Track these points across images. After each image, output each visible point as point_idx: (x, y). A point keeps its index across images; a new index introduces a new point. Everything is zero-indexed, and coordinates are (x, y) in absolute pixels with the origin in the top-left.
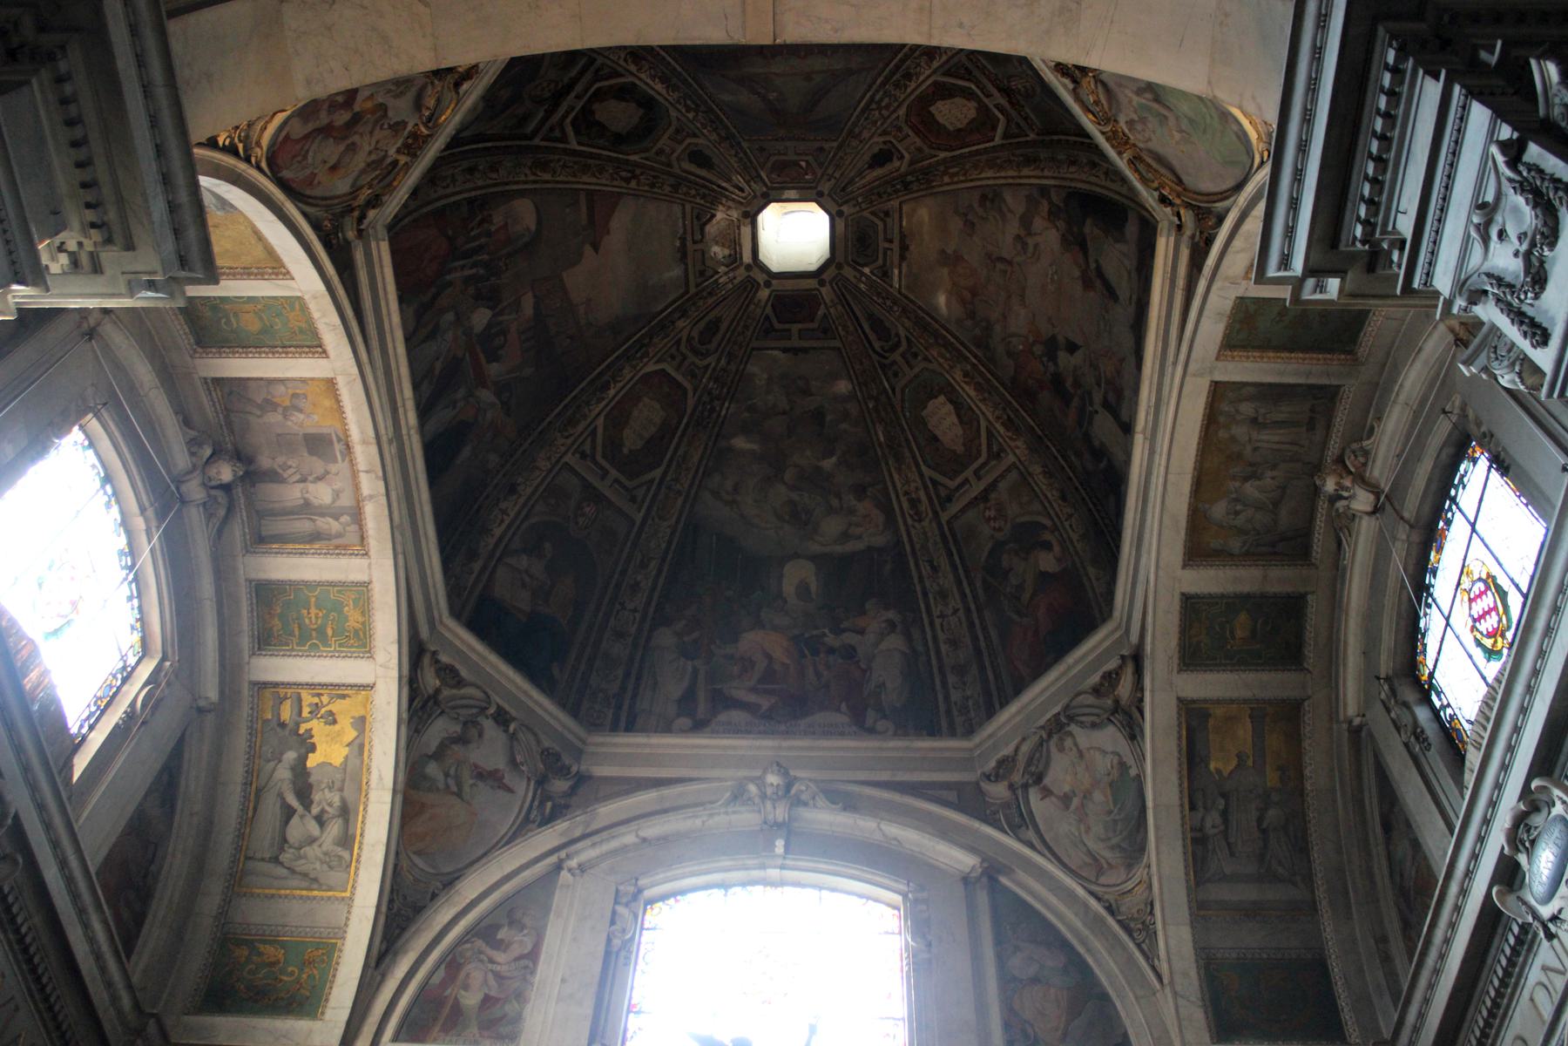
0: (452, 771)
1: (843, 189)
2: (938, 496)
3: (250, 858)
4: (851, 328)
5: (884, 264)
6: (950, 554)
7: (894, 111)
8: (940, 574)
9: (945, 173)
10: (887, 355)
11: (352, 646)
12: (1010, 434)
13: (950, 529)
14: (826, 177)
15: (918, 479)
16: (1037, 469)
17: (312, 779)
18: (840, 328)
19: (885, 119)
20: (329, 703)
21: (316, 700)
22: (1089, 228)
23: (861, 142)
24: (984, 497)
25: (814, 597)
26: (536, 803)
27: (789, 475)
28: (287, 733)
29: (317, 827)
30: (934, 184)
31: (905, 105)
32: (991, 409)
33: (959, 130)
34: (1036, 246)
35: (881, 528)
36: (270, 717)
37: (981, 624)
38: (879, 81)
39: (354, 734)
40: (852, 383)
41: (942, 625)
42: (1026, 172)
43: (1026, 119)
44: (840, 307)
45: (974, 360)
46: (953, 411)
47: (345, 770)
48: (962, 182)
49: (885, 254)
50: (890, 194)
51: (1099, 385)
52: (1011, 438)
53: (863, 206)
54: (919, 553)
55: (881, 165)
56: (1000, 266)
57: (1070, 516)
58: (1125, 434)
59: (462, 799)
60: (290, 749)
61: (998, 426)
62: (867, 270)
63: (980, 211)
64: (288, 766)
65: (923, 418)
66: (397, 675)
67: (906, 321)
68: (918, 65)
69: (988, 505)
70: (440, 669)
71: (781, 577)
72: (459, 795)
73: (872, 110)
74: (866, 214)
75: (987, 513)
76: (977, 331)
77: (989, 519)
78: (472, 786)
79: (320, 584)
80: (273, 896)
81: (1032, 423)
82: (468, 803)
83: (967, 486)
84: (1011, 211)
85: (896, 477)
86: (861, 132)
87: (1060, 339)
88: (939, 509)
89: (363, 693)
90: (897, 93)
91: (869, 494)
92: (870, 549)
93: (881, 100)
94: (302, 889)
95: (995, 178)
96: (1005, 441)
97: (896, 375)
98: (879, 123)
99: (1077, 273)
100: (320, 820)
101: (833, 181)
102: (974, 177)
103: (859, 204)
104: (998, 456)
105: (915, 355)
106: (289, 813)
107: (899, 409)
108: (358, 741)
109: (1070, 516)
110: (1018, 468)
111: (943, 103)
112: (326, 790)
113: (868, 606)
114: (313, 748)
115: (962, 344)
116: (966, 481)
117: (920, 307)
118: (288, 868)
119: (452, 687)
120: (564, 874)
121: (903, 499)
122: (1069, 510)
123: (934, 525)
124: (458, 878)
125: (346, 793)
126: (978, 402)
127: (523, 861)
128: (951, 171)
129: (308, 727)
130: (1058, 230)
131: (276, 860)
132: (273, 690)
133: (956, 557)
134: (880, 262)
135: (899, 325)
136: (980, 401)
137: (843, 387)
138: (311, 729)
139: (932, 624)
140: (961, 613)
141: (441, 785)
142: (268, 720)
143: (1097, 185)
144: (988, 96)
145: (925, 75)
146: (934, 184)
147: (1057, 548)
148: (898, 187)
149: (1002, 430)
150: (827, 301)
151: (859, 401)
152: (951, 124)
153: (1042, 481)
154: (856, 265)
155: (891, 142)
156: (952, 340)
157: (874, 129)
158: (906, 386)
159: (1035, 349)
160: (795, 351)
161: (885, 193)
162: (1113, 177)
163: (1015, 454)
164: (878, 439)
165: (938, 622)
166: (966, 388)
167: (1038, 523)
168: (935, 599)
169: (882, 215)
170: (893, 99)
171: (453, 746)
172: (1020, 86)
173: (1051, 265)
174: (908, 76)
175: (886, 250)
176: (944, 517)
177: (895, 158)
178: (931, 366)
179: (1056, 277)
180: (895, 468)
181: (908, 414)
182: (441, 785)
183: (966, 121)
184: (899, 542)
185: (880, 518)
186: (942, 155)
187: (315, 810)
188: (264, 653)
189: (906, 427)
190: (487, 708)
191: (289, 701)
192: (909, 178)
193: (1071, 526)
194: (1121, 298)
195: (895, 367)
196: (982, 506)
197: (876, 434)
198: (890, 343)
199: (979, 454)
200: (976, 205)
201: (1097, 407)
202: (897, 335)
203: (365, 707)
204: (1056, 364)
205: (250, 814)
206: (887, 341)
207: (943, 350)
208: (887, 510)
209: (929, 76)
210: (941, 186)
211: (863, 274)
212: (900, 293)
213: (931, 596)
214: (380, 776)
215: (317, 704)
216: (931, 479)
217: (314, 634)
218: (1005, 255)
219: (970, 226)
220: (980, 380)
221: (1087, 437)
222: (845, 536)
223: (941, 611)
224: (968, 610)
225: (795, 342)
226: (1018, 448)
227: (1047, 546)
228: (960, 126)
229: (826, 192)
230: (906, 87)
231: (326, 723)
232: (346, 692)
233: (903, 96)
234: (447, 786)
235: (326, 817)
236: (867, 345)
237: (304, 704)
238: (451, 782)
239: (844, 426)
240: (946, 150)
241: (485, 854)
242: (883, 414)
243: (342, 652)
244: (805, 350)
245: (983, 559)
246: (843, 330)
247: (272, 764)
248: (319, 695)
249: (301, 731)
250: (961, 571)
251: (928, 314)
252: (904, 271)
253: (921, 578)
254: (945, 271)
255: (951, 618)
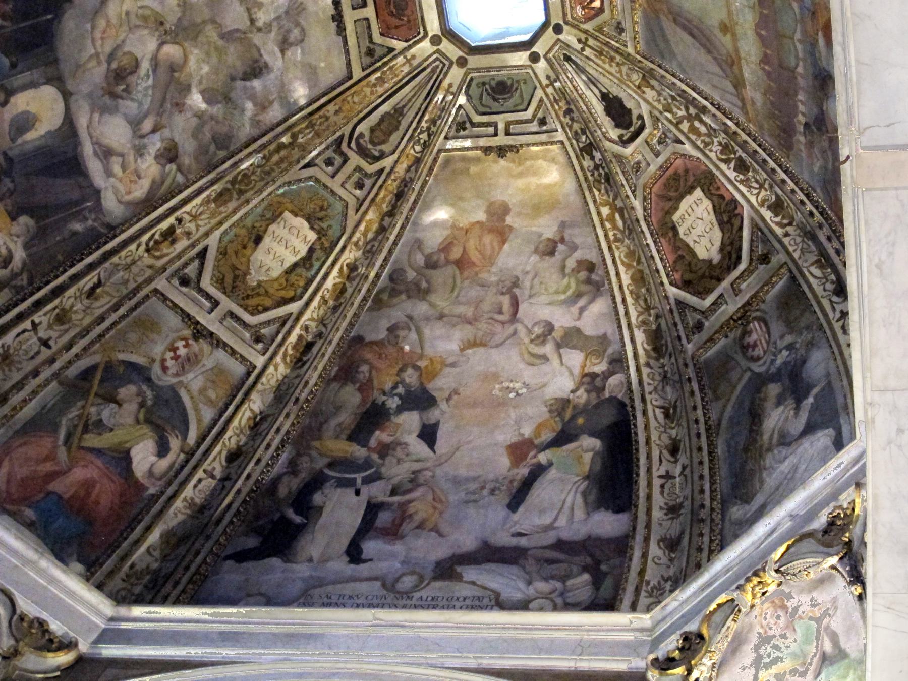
1: (568, 58)
2: (186, 265)
4: (380, 90)
5: (473, 125)
6: (115, 308)
7: (688, 139)
8: (86, 302)
9: (614, 208)
10: (353, 145)
12: (290, 352)
13: (147, 297)
14: (583, 37)
15: (202, 230)
16: (256, 403)
18: (378, 74)
19: (677, 125)
22: (590, 445)
23: (639, 87)
24: (200, 333)
25: (20, 141)
27: (171, 51)
30: (596, 193)
31: (700, 155)
32: (315, 316)
33: (674, 229)
34: (545, 358)
35: (128, 198)
37: (39, 386)
38: (729, 123)
40: (309, 104)
41: (24, 331)
42: (640, 336)
43: (711, 340)
44: (406, 69)
45: (372, 274)
46: (299, 257)
48: (606, 236)
49: (487, 124)
50: (571, 127)
51: (394, 492)
52: (285, 355)
53: (550, 90)
54: (107, 265)
55: (608, 111)
56: (506, 301)
57: (213, 477)
58: (348, 552)
61: (297, 331)
62: (462, 100)
63: (571, 263)
65: (281, 214)
67: (405, 166)
68: (761, 186)
69: (191, 342)
71: (33, 85)
73: (687, 109)
74: (539, 93)
75: (180, 344)
76: (411, 275)
77: (174, 349)
81: (312, 382)
83: (208, 304)
84: (582, 310)
85: (198, 201)
86: (653, 88)
87: (434, 415)
88: (169, 271)
90: (716, 148)
91: (168, 167)
92: (98, 192)
93: (702, 121)
95: (621, 287)
96: (280, 345)
97: (329, 162)
98: (669, 115)
99: (527, 431)
101: (579, 47)
102: (617, 254)
103: (552, 84)
104: (258, 340)
105: (360, 185)
107: (286, 178)
109: (213, 477)
110: (249, 374)
111: (710, 208)
113: (24, 219)
115: (390, 252)
116: (216, 303)
117: (425, 182)
121: (171, 220)
122: (218, 473)
123: (149, 273)
126: (320, 294)
128: (617, 216)
130: (573, 392)
133: (114, 317)
134: (477, 118)
135: (396, 156)
136: (323, 297)
137: (300, 93)
139: (20, 317)
140: (46, 353)
143: (649, 457)
144: (735, 289)
145: (748, 195)
146: (596, 193)
147: (164, 463)
148: (583, 138)
149: (293, 338)
150: (413, 51)
151: (286, 119)
152: (682, 218)
153: (243, 418)
154: (468, 85)
155: (642, 128)
156: (392, 238)
157: (660, 108)
158: (317, 180)
159: (410, 371)
160: (338, 18)
161: (572, 119)
162: (667, 486)
163: (265, 368)
164: (241, 161)
165: (27, 325)
166: (335, 272)
167: (187, 430)
168: (55, 309)
169: (540, 115)
170: (707, 140)
172: (754, 337)
173: (526, 385)
174: (742, 167)
175: (495, 124)
176: (161, 284)
177: (619, 131)
178: (351, 212)
179: (512, 395)
180: (208, 196)
181: (281, 191)
183: (689, 240)
184: (113, 230)
185: (140, 191)
186: (637, 204)
189: (265, 194)
192: (598, 155)
193: (200, 481)
194: (516, 517)
195: (338, 160)
196: (187, 332)
197: (250, 155)
198: (370, 146)
199: (254, 312)
200: (578, 255)
201: (365, 490)
202: (382, 156)
204: (400, 410)
206: (372, 142)
207: (375, 227)
208: (149, 203)
209: (748, 201)
210: (595, 201)
211: (456, 95)
212: (439, 151)
213: (56, 302)
216: (205, 249)
218: (522, 308)
219: (549, 249)
220: (347, 294)
221: (316, 482)
222: (106, 153)
223: (40, 323)
224: (52, 361)
225: (350, 16)
226: (276, 369)
227: (163, 450)
228: (681, 231)
229: (561, 37)
230: (727, 161)
233: (712, 155)
236: (361, 115)
239: (249, 105)
240: (645, 210)
242: (276, 158)
244: (341, 30)
245: (122, 356)
246: (377, 79)
250: (98, 330)
251: (419, 194)
252: (469, 153)
253: (75, 278)
254: (481, 216)
255: (35, 339)
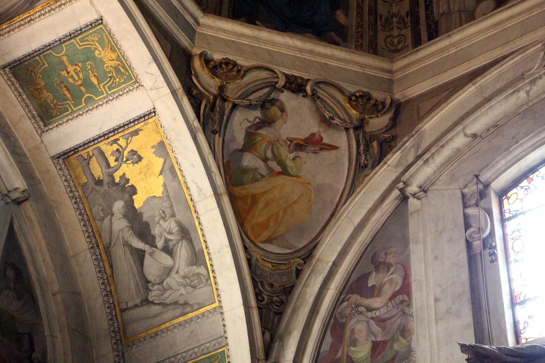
0: (269, 154)
3: (125, 310)
11: (120, 84)
17: (145, 218)
20: (127, 144)
21: (115, 147)
26: (362, 148)
28: (106, 187)
29: (168, 257)
36: (86, 181)
39: (161, 160)
47: (168, 196)
59: (289, 174)
60: (116, 200)
64: (121, 216)
66: (168, 91)
70: (215, 67)
72: (285, 172)
78: (294, 159)
79: (61, 41)
80: (156, 334)
82: (297, 176)
89: (150, 121)
94: (177, 317)
100: (168, 250)
106: (140, 255)
108: (167, 166)
112: (162, 222)
114: (133, 191)
118: (159, 304)
119: (235, 78)
120: (412, 201)
124: (315, 247)
125: (178, 217)
127: (369, 206)
129: (121, 174)
131: (146, 302)
132: (77, 155)
138: (124, 174)
141: (264, 171)
142: (85, 184)
171: (260, 131)
182: (264, 171)
187: (160, 243)
188: (51, 127)
190: (277, 83)
191: (94, 159)
203: (158, 132)
205: (108, 271)
214: (198, 187)
215: (118, 150)
217: (82, 88)
231: (133, 163)
232: (137, 127)
234: (271, 170)
235: (171, 244)
237: (108, 155)
238: (273, 165)
241: (332, 215)
243: (114, 93)
247: (107, 220)
248: (116, 141)
249: (117, 180)
